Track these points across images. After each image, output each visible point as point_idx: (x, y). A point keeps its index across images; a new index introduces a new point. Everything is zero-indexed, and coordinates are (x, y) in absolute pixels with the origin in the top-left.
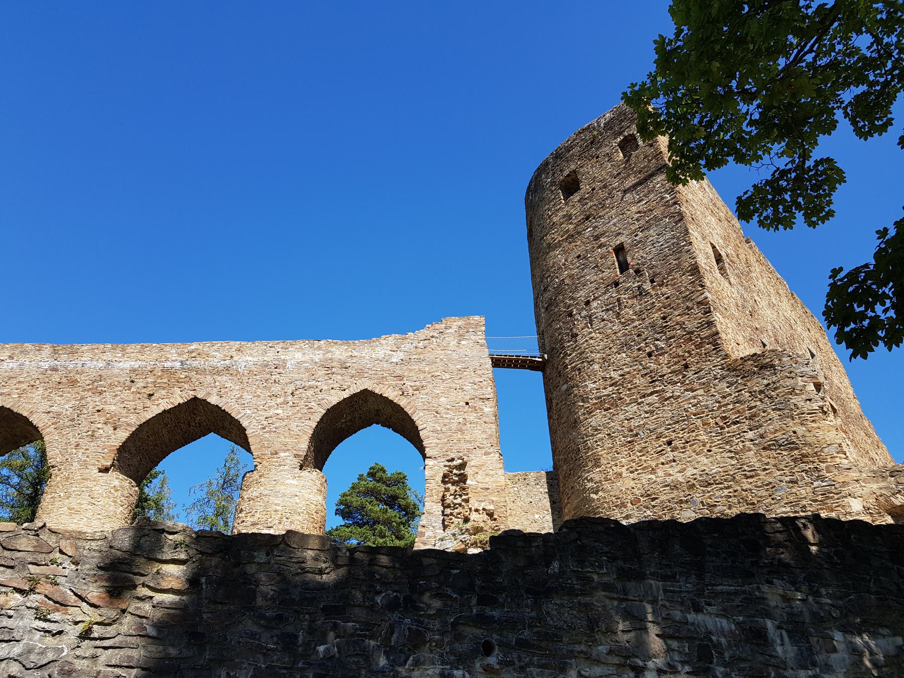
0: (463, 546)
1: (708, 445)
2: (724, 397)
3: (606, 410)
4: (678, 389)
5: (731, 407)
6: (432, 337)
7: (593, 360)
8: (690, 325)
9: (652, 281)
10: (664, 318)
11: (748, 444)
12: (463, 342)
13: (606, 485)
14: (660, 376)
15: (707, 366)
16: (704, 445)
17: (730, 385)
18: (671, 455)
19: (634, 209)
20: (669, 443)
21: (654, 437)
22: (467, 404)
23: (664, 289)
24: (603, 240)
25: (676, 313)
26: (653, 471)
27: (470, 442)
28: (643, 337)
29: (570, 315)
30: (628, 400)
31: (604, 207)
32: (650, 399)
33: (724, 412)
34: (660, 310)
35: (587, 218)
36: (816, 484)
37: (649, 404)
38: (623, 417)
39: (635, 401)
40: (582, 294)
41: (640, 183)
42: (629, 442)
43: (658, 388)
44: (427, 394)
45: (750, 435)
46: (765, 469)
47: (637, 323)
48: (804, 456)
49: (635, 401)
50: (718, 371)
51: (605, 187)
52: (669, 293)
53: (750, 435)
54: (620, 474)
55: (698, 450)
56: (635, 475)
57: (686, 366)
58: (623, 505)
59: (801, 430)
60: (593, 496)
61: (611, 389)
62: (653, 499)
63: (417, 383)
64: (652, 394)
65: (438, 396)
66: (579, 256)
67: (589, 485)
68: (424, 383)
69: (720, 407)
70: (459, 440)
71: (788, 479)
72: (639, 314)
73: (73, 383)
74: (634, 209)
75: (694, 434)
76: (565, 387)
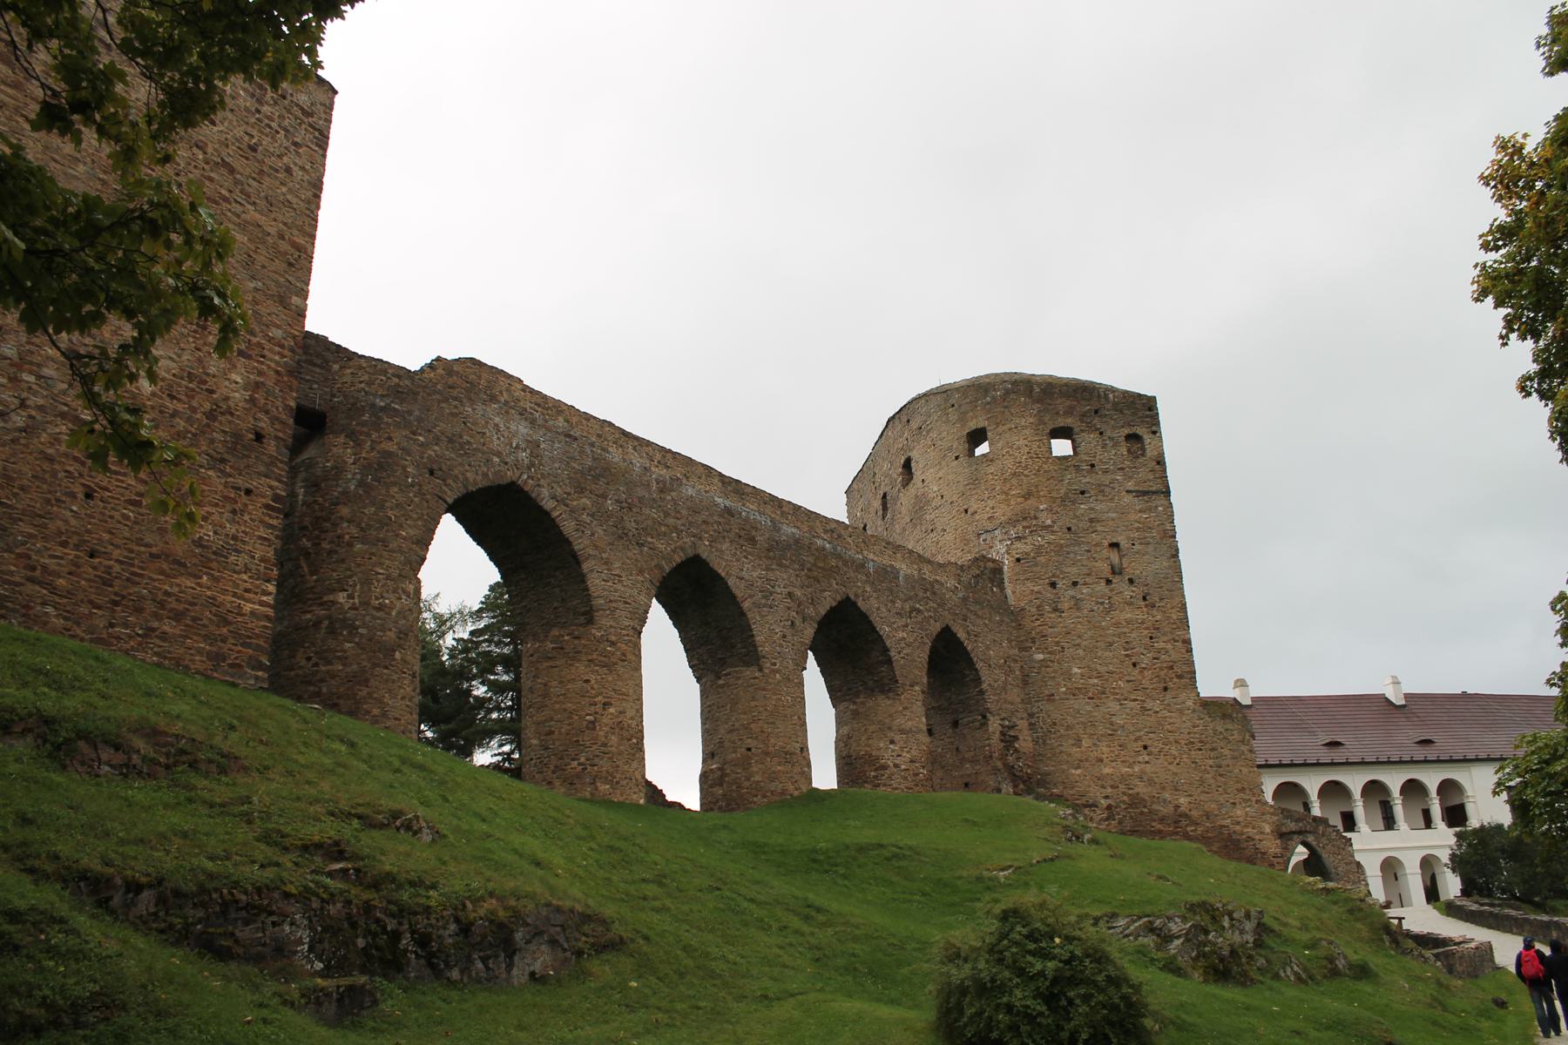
8: (1174, 656)
9: (1144, 599)
15: (1183, 696)
19: (1133, 517)
20: (1145, 747)
29: (1053, 585)
35: (1083, 493)
41: (1145, 493)
45: (1211, 762)
50: (1190, 703)
51: (1105, 472)
53: (1211, 762)
57: (1166, 689)
58: (1103, 787)
72: (1128, 622)
73: (752, 540)
76: (1041, 657)
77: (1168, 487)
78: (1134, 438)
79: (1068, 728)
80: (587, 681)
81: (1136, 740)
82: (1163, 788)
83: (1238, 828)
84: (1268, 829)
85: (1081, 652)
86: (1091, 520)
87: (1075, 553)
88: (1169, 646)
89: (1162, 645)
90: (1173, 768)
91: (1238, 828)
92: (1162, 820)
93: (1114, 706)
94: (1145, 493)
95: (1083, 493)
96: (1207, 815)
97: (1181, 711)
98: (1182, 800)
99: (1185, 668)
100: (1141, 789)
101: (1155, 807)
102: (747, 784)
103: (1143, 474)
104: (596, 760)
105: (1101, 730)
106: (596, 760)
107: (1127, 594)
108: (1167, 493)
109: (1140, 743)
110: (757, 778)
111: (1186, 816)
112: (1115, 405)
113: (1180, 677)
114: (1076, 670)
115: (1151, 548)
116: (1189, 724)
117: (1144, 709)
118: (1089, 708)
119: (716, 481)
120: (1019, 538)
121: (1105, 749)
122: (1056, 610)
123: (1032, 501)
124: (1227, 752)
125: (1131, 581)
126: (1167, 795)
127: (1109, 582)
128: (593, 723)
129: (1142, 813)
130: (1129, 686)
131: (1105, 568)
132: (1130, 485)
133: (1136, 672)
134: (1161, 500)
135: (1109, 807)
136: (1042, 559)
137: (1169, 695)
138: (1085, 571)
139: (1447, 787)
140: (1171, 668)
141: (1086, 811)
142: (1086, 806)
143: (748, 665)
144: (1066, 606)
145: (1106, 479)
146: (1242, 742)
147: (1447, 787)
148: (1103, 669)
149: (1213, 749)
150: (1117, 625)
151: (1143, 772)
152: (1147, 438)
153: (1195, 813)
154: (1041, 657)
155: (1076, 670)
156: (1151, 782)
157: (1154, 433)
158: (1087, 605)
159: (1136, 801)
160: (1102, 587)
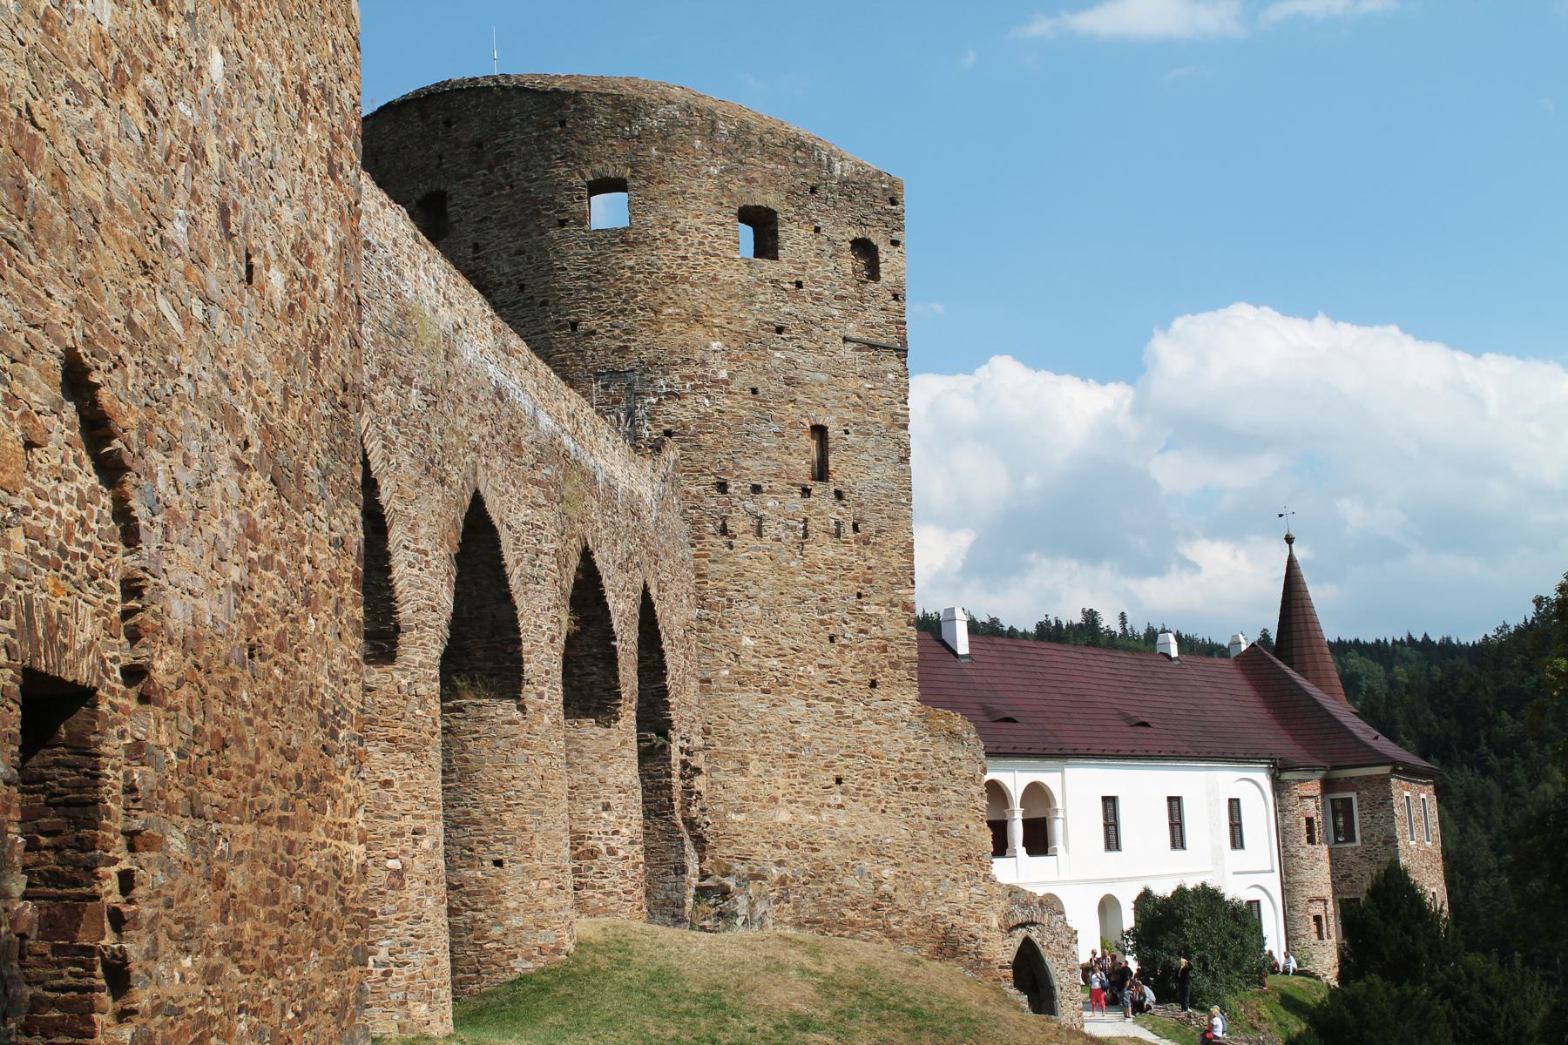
5: (912, 765)
9: (855, 528)
11: (925, 821)
13: (755, 806)
19: (851, 385)
21: (823, 763)
23: (868, 553)
24: (800, 397)
26: (816, 812)
28: (829, 605)
29: (722, 487)
32: (826, 707)
34: (855, 579)
35: (780, 330)
36: (973, 890)
37: (823, 714)
38: (785, 714)
40: (754, 467)
41: (873, 346)
42: (791, 756)
43: (835, 696)
45: (927, 811)
47: (823, 578)
48: (969, 856)
51: (818, 298)
52: (872, 563)
53: (927, 811)
54: (775, 799)
56: (793, 807)
57: (873, 684)
58: (779, 847)
59: (973, 826)
61: (775, 662)
62: (814, 850)
64: (829, 699)
67: (728, 796)
69: (901, 761)
77: (904, 341)
78: (864, 248)
80: (387, 784)
81: (828, 767)
82: (862, 851)
86: (789, 381)
91: (958, 920)
92: (854, 905)
93: (798, 707)
94: (873, 346)
95: (780, 330)
96: (918, 895)
98: (886, 873)
100: (829, 852)
102: (496, 932)
103: (873, 315)
104: (406, 955)
105: (778, 747)
106: (406, 955)
109: (833, 774)
110: (515, 921)
112: (844, 182)
114: (747, 641)
116: (902, 746)
118: (762, 708)
119: (1353, 653)
120: (671, 395)
121: (782, 781)
123: (699, 331)
125: (839, 495)
126: (866, 864)
127: (806, 492)
128: (398, 874)
130: (821, 676)
132: (852, 329)
133: (833, 650)
134: (895, 364)
135: (782, 881)
136: (708, 440)
137: (879, 693)
138: (773, 469)
139: (1036, 792)
143: (502, 695)
145: (816, 313)
147: (1036, 792)
148: (786, 643)
150: (811, 568)
157: (895, 243)
158: (771, 529)
160: (795, 502)
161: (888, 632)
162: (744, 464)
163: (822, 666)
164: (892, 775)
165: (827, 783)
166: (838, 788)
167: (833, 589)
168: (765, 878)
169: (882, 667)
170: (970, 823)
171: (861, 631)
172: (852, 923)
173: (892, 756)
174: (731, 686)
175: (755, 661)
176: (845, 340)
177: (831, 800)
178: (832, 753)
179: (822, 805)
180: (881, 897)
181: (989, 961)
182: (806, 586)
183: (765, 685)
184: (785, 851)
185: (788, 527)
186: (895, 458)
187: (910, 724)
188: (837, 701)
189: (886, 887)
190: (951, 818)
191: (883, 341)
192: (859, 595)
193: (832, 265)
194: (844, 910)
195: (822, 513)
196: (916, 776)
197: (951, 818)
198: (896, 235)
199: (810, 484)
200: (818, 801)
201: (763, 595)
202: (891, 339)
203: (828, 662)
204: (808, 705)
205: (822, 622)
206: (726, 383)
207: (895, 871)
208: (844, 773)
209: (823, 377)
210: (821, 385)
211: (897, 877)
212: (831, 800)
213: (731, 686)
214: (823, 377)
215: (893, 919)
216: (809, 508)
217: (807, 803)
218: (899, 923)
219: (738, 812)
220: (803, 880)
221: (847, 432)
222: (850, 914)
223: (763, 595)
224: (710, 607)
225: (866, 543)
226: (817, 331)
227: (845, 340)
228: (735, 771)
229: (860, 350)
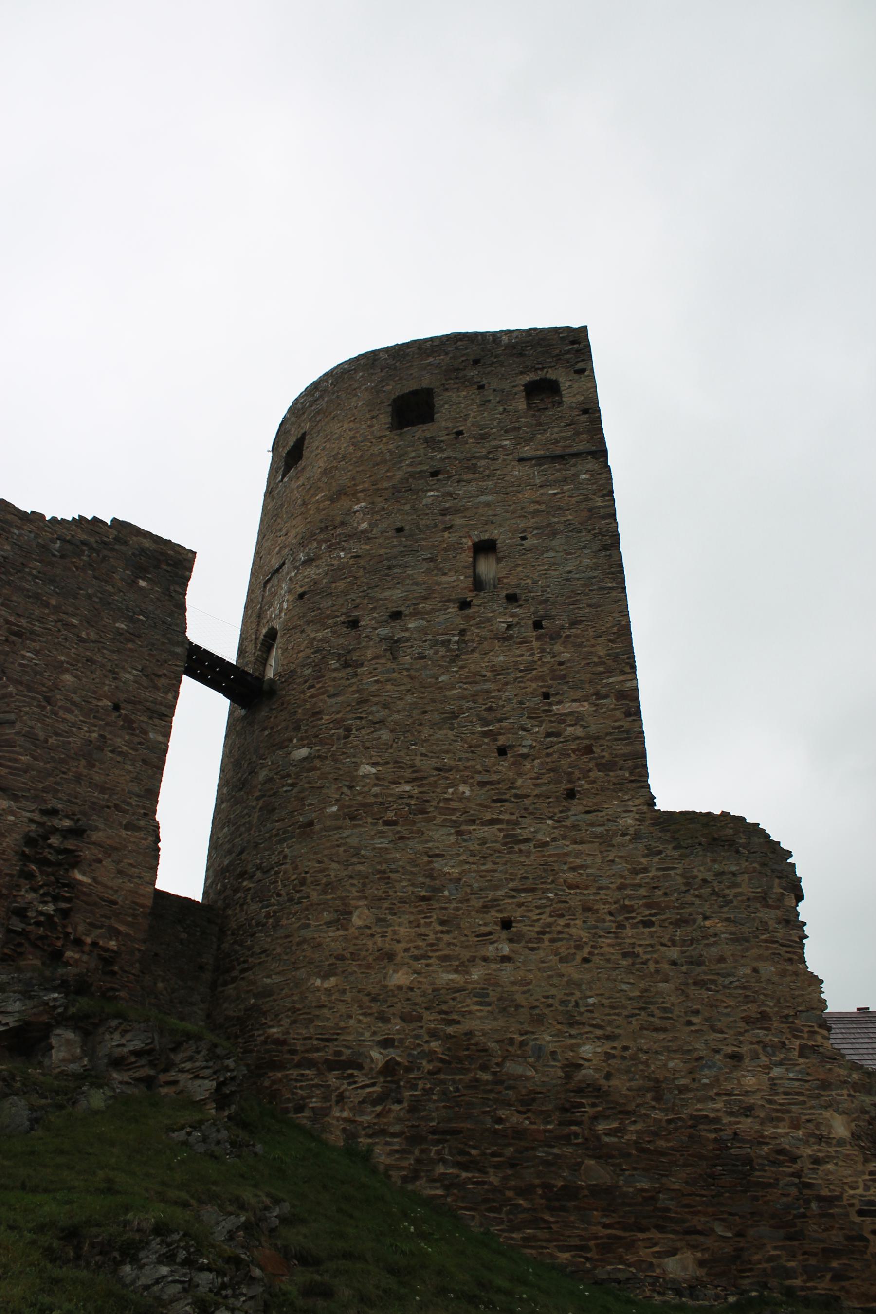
0: (45, 1018)
1: (587, 949)
2: (635, 872)
3: (387, 823)
4: (545, 830)
5: (643, 892)
6: (84, 543)
7: (382, 722)
9: (537, 625)
10: (546, 696)
12: (142, 583)
14: (516, 796)
15: (613, 806)
16: (579, 947)
17: (651, 852)
18: (506, 949)
20: (506, 924)
22: (116, 707)
25: (573, 694)
26: (462, 968)
27: (103, 790)
29: (354, 624)
30: (439, 819)
31: (473, 469)
32: (485, 831)
33: (629, 897)
35: (435, 474)
36: (776, 1072)
37: (483, 842)
39: (455, 824)
42: (423, 899)
43: (506, 817)
44: (37, 652)
45: (674, 953)
46: (689, 1023)
48: (764, 1016)
49: (455, 824)
53: (674, 953)
55: (563, 952)
57: (571, 794)
58: (383, 1018)
60: (318, 982)
63: (23, 622)
64: (492, 822)
65: (60, 668)
66: (400, 530)
68: (37, 627)
69: (621, 888)
70: (78, 778)
71: (729, 1050)
72: (497, 671)
74: (528, 494)
75: (562, 922)
76: (304, 752)
79: (329, 887)
81: (485, 908)
82: (539, 1020)
83: (746, 1124)
84: (840, 1128)
85: (385, 735)
86: (444, 512)
87: (406, 566)
88: (585, 707)
89: (567, 707)
90: (571, 971)
91: (746, 1124)
93: (441, 837)
97: (605, 841)
98: (587, 1050)
99: (622, 748)
100: (480, 1023)
101: (511, 1067)
107: (501, 623)
108: (601, 453)
109: (495, 915)
111: (595, 1091)
113: (606, 767)
114: (367, 769)
115: (558, 542)
116: (621, 866)
117: (512, 841)
118: (380, 843)
120: (309, 561)
122: (346, 665)
123: (345, 502)
124: (715, 925)
127: (465, 605)
129: (475, 1084)
131: (456, 581)
132: (527, 450)
133: (504, 766)
135: (390, 1068)
136: (341, 585)
137: (576, 807)
140: (589, 750)
141: (332, 1079)
142: (332, 1065)
144: (370, 654)
146: (764, 899)
148: (426, 765)
149: (678, 923)
151: (491, 981)
152: (565, 383)
153: (619, 1083)
154: (304, 752)
155: (367, 769)
156: (507, 1006)
159: (464, 1053)
161: (592, 729)
162: (382, 596)
163: (482, 784)
164: (604, 908)
165: (487, 929)
166: (504, 935)
167: (505, 695)
168: (360, 1067)
169: (585, 774)
170: (760, 965)
171: (549, 735)
172: (519, 1133)
173: (604, 882)
174: (339, 823)
175: (376, 790)
176: (521, 460)
177: (490, 950)
178: (496, 888)
179: (473, 959)
180: (579, 1091)
181: (831, 1200)
182: (464, 698)
183: (390, 815)
184: (397, 1025)
185: (435, 643)
186: (595, 547)
187: (637, 837)
188: (508, 822)
189: (588, 1072)
190: (722, 959)
191: (575, 450)
192: (546, 696)
193: (501, 409)
194: (502, 1113)
195: (488, 620)
196: (649, 906)
197: (722, 959)
198: (580, 366)
199: (469, 596)
200: (466, 955)
201: (396, 716)
202: (581, 446)
203: (495, 777)
204: (459, 833)
205: (485, 734)
206: (363, 532)
207: (607, 1047)
208: (518, 914)
209: (490, 498)
210: (487, 504)
211: (608, 1056)
212: (490, 950)
213: (339, 823)
214: (490, 498)
215: (601, 1127)
216: (468, 618)
217: (445, 958)
218: (609, 1133)
219: (325, 977)
220: (427, 1066)
221: (524, 538)
222: (514, 1118)
223: (396, 716)
224: (322, 743)
225: (554, 637)
226: (483, 463)
227: (521, 460)
228: (329, 924)
229: (540, 465)
